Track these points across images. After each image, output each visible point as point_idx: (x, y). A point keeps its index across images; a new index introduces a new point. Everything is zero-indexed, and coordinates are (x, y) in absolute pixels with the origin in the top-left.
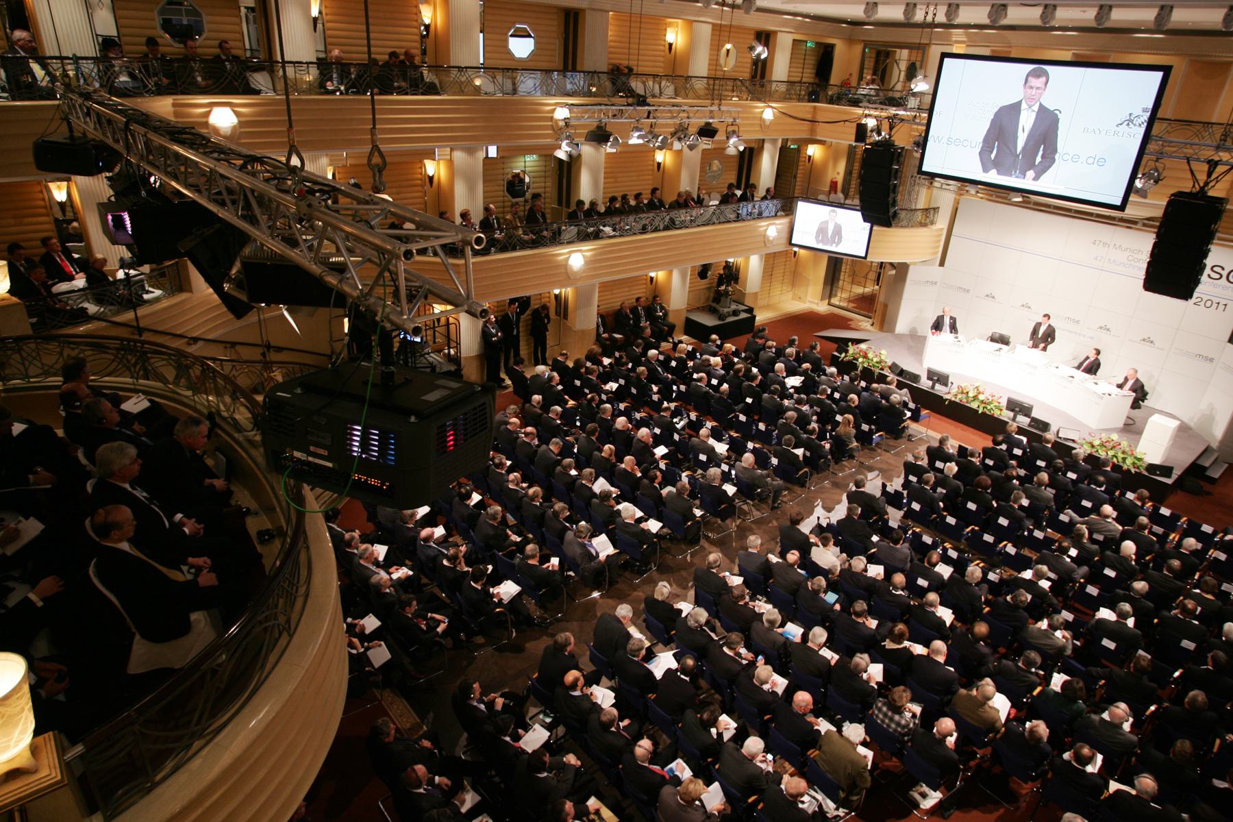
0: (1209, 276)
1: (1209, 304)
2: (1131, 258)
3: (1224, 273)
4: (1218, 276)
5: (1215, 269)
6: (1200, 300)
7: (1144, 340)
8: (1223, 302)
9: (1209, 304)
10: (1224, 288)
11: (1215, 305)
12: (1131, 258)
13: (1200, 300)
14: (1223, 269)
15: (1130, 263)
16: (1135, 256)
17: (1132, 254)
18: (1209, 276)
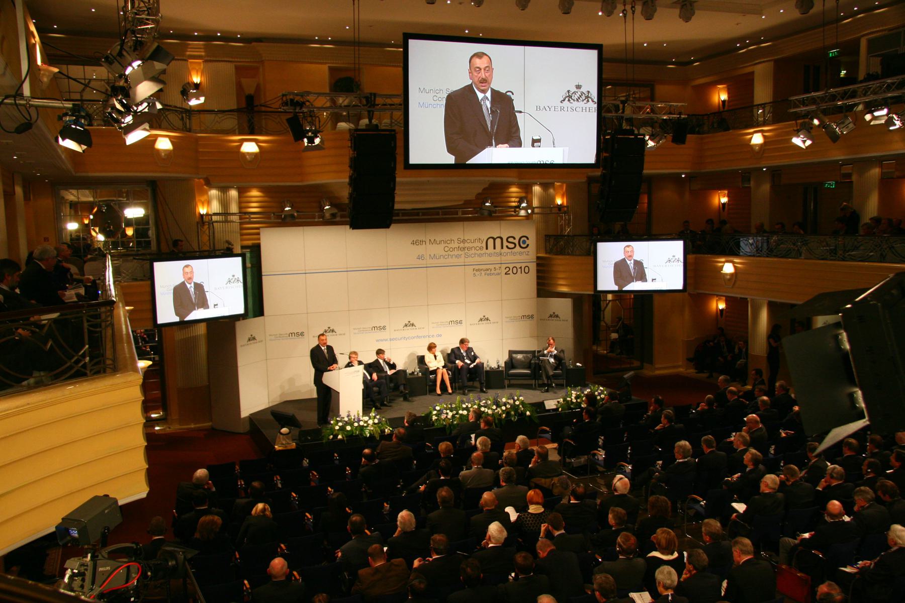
0: (507, 247)
1: (515, 271)
2: (446, 249)
3: (516, 241)
4: (512, 246)
5: (511, 240)
6: (508, 269)
7: (481, 320)
8: (523, 265)
9: (515, 271)
10: (521, 254)
11: (519, 270)
12: (446, 249)
13: (508, 269)
14: (514, 238)
15: (447, 253)
16: (450, 246)
17: (447, 245)
18: (507, 247)
